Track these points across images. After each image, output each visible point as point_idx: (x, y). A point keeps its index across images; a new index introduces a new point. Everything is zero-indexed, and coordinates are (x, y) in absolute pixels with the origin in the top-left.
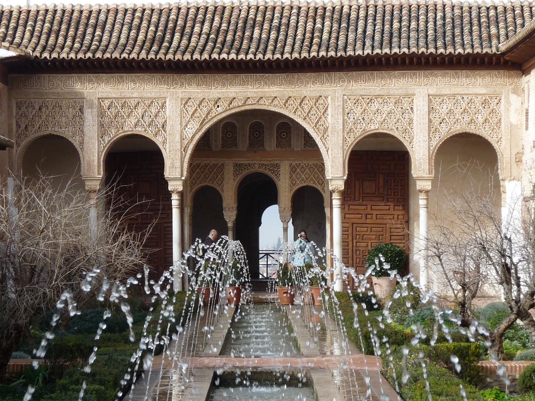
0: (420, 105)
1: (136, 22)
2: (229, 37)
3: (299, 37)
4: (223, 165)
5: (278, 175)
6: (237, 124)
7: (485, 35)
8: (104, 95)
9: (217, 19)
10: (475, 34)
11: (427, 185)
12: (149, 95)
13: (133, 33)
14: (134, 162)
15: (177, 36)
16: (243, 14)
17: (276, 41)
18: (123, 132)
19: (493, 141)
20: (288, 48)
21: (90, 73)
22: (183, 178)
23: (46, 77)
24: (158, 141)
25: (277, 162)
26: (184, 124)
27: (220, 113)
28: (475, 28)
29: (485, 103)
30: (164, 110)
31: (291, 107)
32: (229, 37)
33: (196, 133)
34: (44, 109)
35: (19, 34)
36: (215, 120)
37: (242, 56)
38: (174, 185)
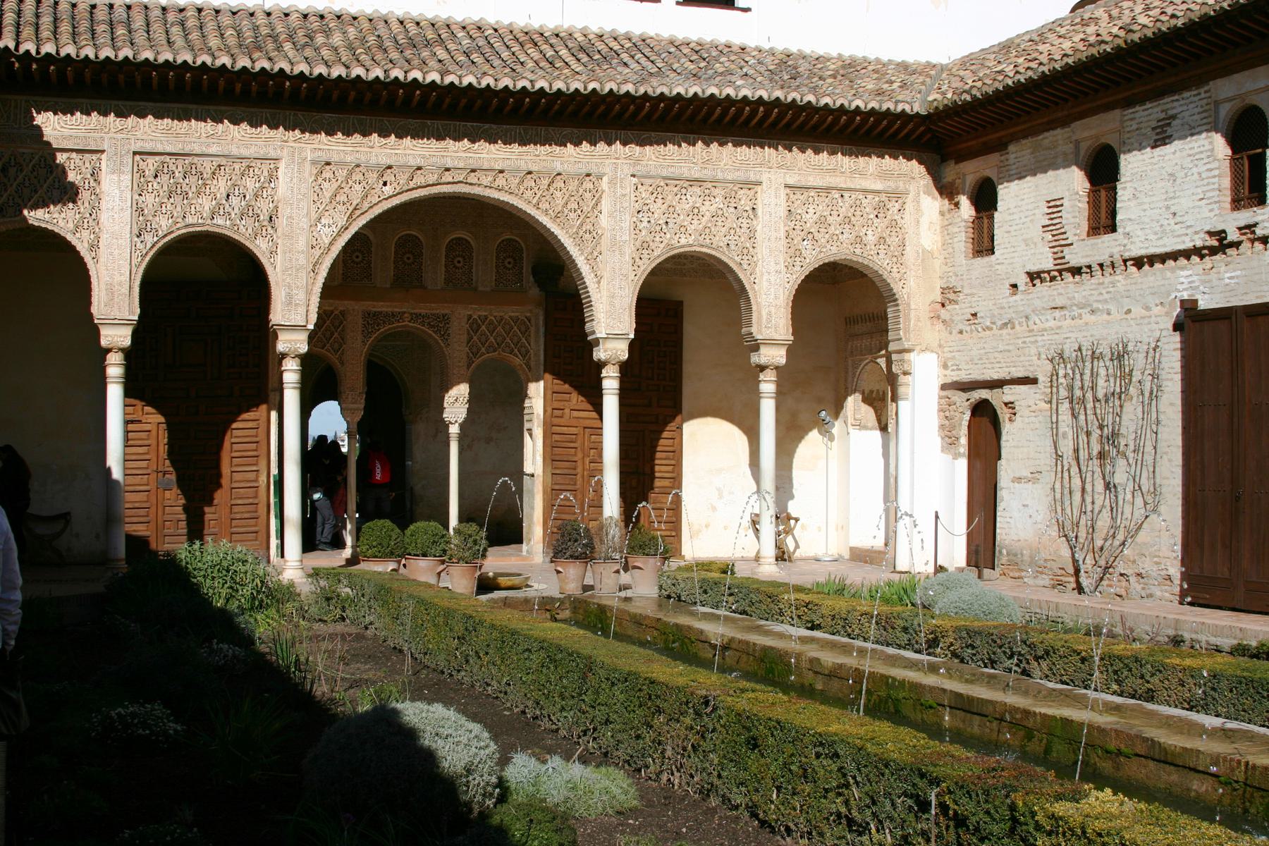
0: (771, 203)
4: (343, 313)
5: (445, 336)
6: (371, 237)
8: (148, 147)
11: (777, 356)
12: (245, 153)
14: (206, 287)
18: (187, 226)
21: (118, 99)
22: (311, 327)
24: (260, 248)
25: (446, 311)
26: (314, 216)
27: (386, 197)
29: (880, 209)
30: (272, 185)
31: (529, 194)
33: (339, 235)
34: (12, 171)
36: (377, 211)
38: (290, 341)
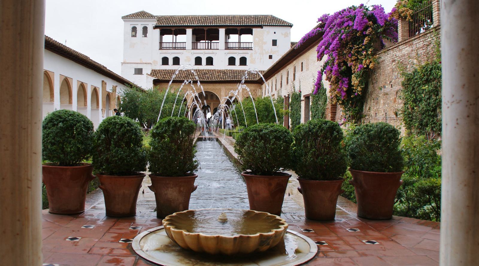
1: (182, 73)
2: (201, 76)
3: (216, 76)
7: (254, 77)
9: (199, 73)
10: (252, 77)
13: (181, 75)
15: (190, 76)
16: (204, 72)
17: (211, 77)
20: (213, 79)
23: (163, 84)
28: (252, 75)
32: (201, 76)
35: (158, 75)
37: (204, 80)
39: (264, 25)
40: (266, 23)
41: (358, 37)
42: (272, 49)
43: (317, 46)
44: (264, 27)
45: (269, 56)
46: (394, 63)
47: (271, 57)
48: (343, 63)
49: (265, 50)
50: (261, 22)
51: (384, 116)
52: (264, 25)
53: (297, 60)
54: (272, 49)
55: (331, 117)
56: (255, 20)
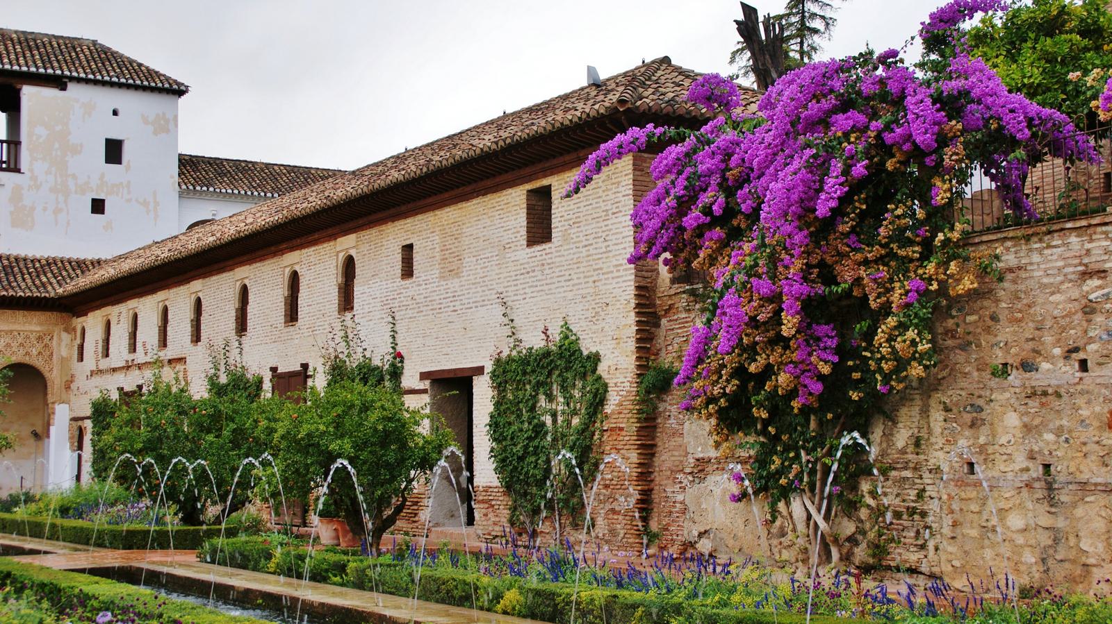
19: (45, 370)
29: (39, 339)
39: (72, 79)
40: (80, 70)
41: (889, 174)
42: (102, 176)
43: (529, 186)
44: (71, 86)
45: (94, 200)
46: (1096, 282)
47: (98, 206)
48: (816, 270)
49: (74, 177)
50: (56, 64)
51: (1036, 471)
52: (72, 79)
53: (371, 234)
54: (102, 176)
55: (640, 465)
56: (28, 54)
